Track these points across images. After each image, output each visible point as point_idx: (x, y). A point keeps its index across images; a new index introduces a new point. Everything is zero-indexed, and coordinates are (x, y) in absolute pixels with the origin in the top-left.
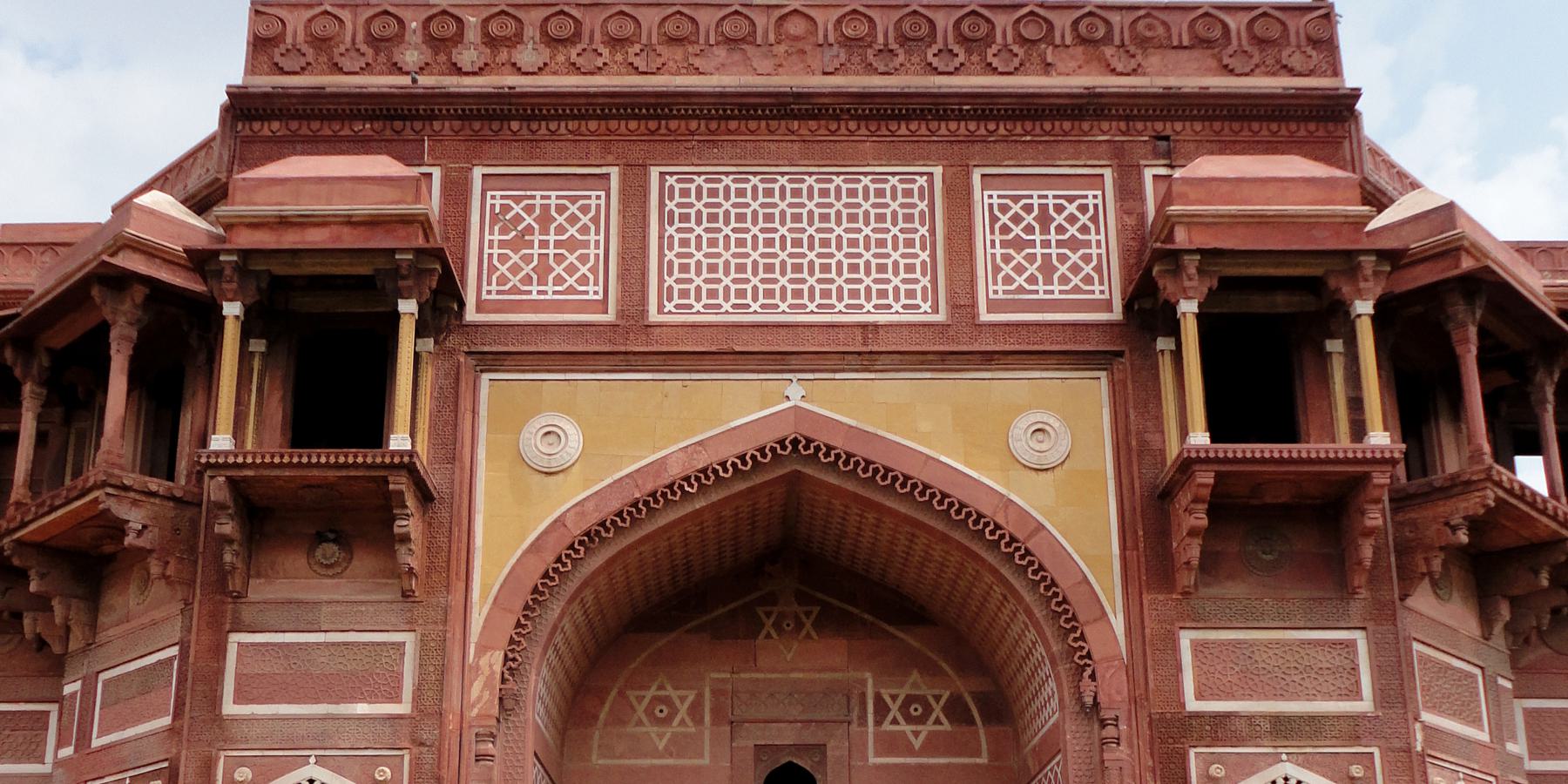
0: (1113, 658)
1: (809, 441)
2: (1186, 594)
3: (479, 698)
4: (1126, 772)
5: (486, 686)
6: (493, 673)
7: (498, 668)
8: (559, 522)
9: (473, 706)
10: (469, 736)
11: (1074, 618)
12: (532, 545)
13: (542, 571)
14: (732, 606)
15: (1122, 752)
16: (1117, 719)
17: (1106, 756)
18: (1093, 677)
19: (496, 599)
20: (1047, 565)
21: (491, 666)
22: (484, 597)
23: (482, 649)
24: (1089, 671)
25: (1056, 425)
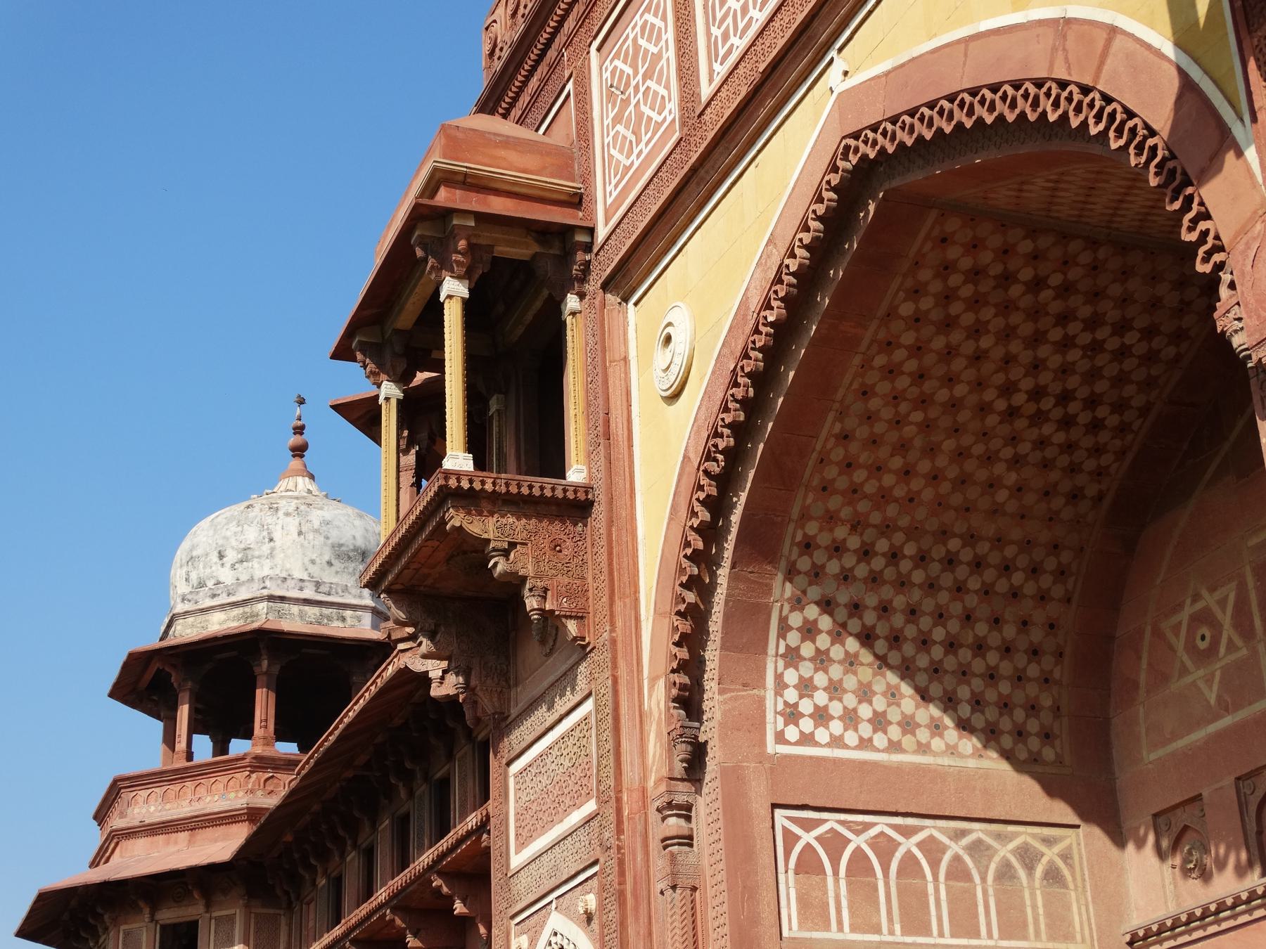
18: (1232, 286)
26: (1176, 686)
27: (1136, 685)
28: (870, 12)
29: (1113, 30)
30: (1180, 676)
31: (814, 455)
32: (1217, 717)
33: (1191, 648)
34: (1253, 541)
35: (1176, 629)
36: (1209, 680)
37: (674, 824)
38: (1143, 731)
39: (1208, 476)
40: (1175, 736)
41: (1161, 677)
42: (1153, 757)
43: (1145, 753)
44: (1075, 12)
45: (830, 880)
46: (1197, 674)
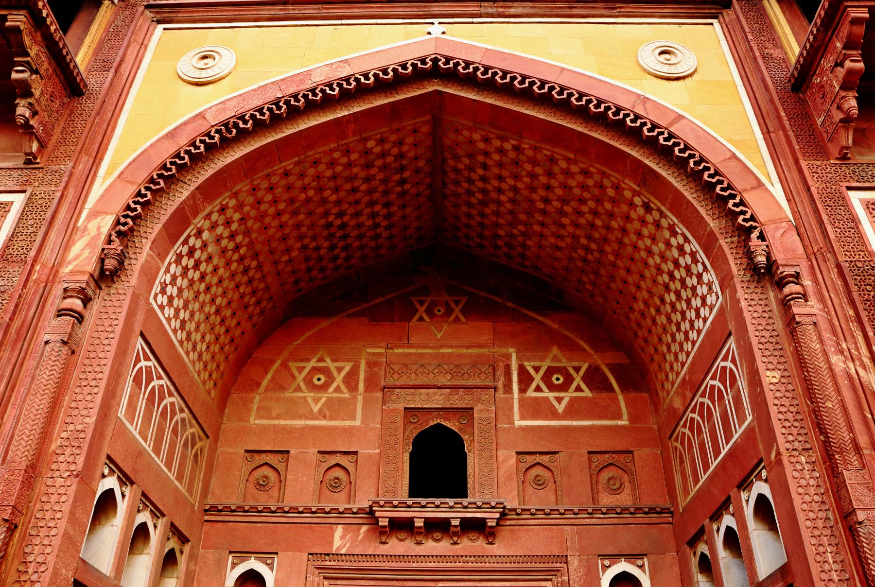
0: (781, 220)
1: (448, 60)
2: (844, 158)
3: (78, 256)
4: (823, 325)
5: (88, 244)
6: (99, 234)
7: (105, 230)
8: (201, 116)
9: (70, 263)
10: (58, 290)
11: (730, 187)
12: (170, 132)
13: (173, 150)
14: (389, 296)
15: (814, 306)
16: (797, 276)
17: (795, 310)
18: (762, 237)
19: (122, 173)
20: (692, 143)
21: (99, 228)
22: (108, 173)
23: (95, 214)
24: (755, 235)
25: (680, 48)
26: (288, 394)
27: (258, 385)
28: (472, 23)
29: (683, 117)
30: (295, 391)
31: (270, 170)
32: (315, 418)
33: (308, 381)
34: (372, 350)
35: (300, 370)
36: (316, 401)
37: (76, 303)
38: (255, 407)
39: (349, 312)
40: (278, 417)
41: (278, 386)
42: (257, 422)
43: (252, 418)
44: (647, 96)
45: (142, 395)
46: (310, 395)
